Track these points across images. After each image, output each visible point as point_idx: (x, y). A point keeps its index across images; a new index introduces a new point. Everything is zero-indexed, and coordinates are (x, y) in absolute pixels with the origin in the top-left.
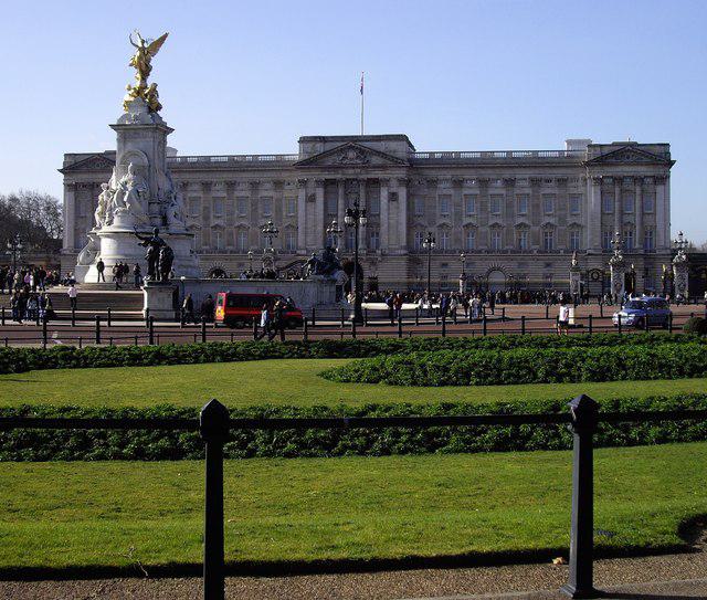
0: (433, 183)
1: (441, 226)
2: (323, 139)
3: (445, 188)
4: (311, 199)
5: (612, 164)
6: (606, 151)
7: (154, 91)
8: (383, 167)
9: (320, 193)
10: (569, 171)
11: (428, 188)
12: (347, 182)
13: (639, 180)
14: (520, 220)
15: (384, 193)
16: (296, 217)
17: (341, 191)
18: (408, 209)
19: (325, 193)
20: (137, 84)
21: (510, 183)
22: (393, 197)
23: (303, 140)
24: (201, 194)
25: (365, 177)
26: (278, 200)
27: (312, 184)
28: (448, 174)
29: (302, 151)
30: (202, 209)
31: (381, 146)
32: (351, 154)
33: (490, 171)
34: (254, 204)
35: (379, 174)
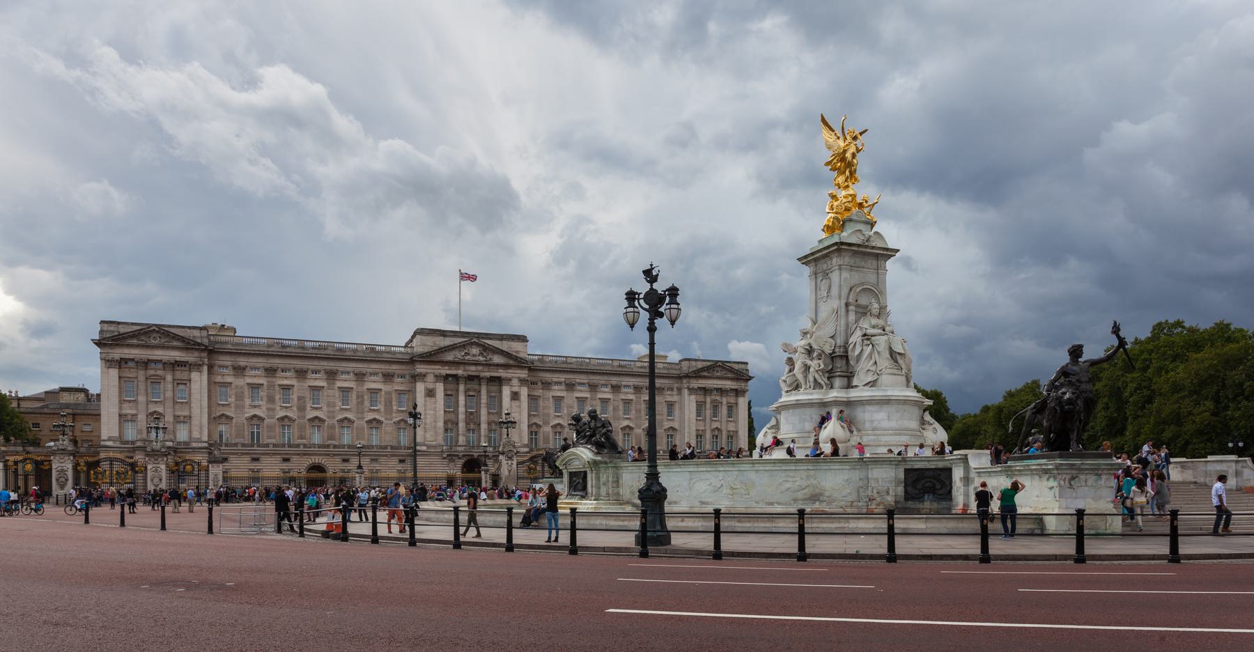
0: (547, 385)
1: (554, 427)
2: (443, 333)
3: (558, 391)
4: (430, 393)
5: (705, 377)
6: (700, 365)
8: (506, 366)
9: (440, 388)
10: (666, 381)
12: (470, 378)
13: (721, 391)
14: (626, 423)
15: (506, 391)
21: (616, 388)
22: (515, 396)
24: (293, 382)
25: (488, 374)
27: (430, 378)
28: (562, 377)
30: (295, 397)
31: (504, 346)
32: (475, 351)
33: (597, 377)
34: (360, 397)
35: (502, 373)
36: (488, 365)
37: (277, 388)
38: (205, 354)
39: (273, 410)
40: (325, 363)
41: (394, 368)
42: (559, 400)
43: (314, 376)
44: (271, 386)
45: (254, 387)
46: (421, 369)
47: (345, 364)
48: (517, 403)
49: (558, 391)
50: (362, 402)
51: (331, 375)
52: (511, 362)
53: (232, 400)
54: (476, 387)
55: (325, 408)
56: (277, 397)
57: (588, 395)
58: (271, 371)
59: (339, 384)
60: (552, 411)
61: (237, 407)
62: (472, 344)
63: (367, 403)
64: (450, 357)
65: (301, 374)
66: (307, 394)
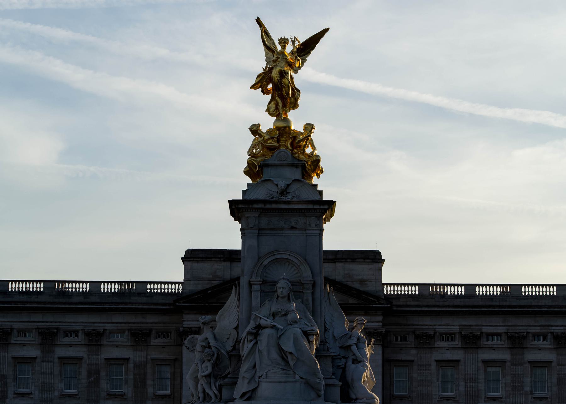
0: (426, 340)
11: (416, 348)
20: (267, 123)
23: (192, 257)
28: (453, 325)
33: (525, 321)
40: (38, 317)
47: (70, 318)
51: (48, 337)
57: (506, 356)
59: (61, 352)
63: (104, 384)
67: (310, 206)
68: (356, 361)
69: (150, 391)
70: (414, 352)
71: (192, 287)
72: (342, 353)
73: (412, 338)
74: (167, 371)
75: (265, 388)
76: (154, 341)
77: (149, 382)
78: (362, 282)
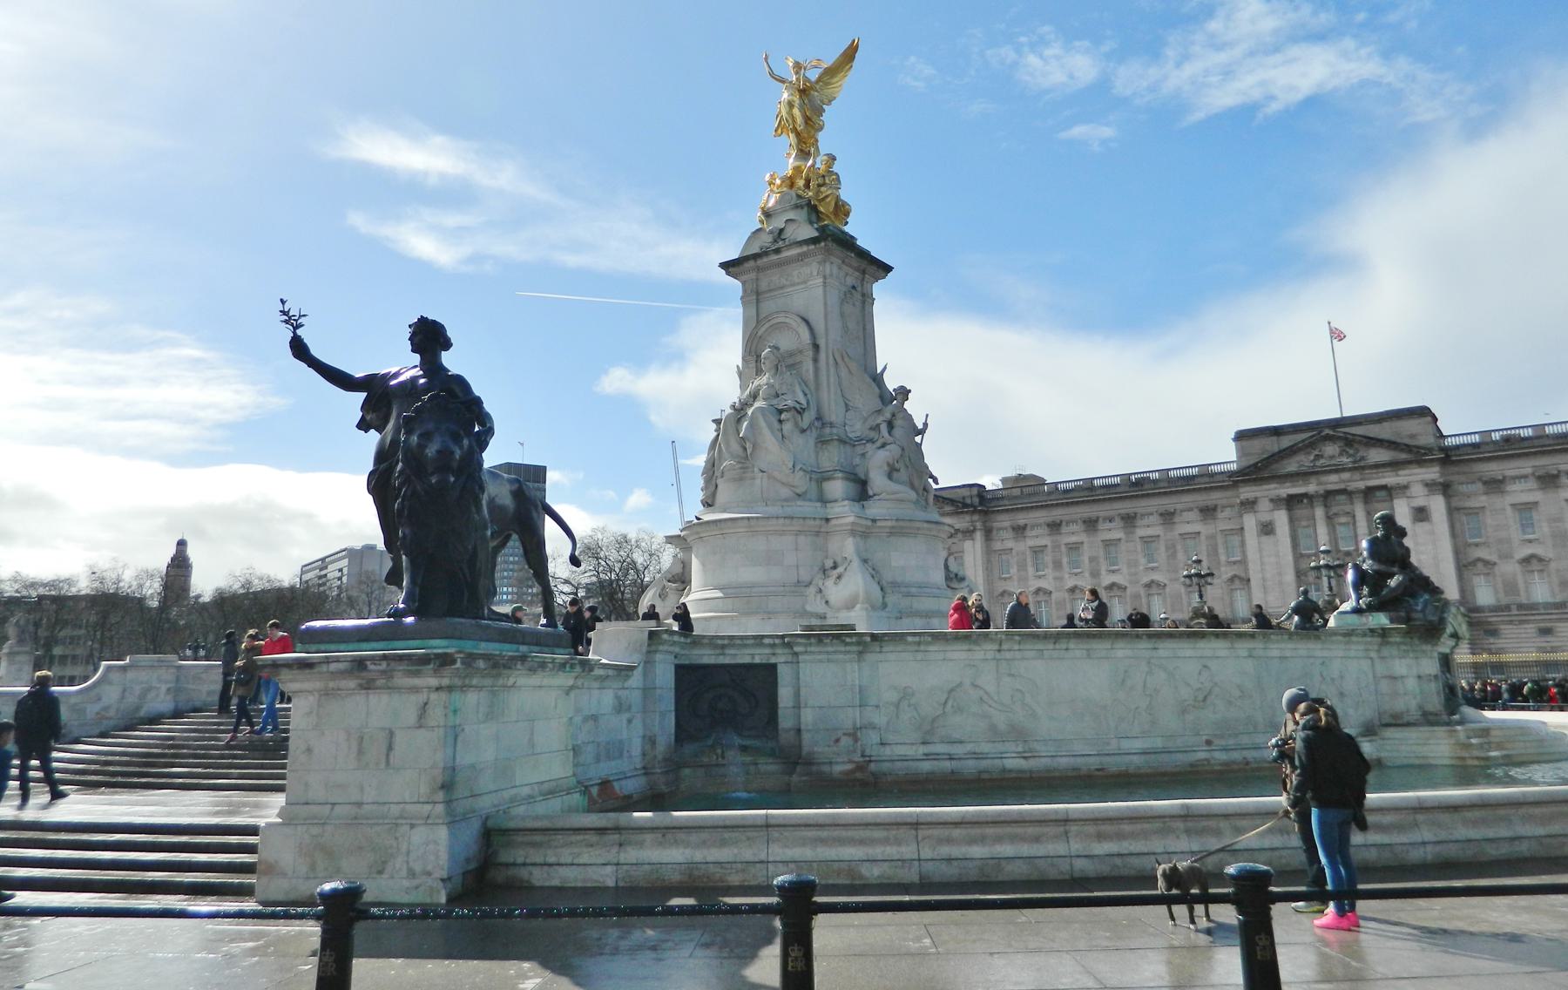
0: (1495, 485)
1: (1527, 560)
2: (1276, 431)
3: (1522, 492)
4: (1267, 529)
7: (828, 178)
8: (1394, 465)
9: (1281, 518)
12: (1328, 496)
16: (1243, 562)
17: (1319, 512)
18: (1453, 535)
19: (1291, 520)
22: (1421, 514)
23: (1242, 436)
24: (1083, 537)
25: (1361, 485)
26: (1212, 537)
27: (1264, 505)
28: (1526, 466)
29: (1242, 453)
30: (1086, 559)
32: (1330, 449)
34: (1172, 550)
35: (1389, 479)
36: (1359, 468)
37: (1063, 548)
38: (976, 517)
39: (1060, 579)
41: (1215, 497)
42: (1525, 509)
43: (1108, 525)
44: (1056, 547)
45: (1037, 551)
46: (1247, 492)
48: (1425, 526)
49: (1522, 492)
50: (1173, 555)
51: (1129, 520)
52: (1403, 456)
53: (1014, 571)
54: (1347, 508)
55: (1125, 570)
56: (1065, 560)
58: (1055, 527)
60: (1515, 534)
61: (1020, 580)
62: (1328, 438)
63: (1181, 556)
64: (1291, 466)
65: (1091, 524)
66: (1101, 553)
67: (805, 248)
68: (883, 446)
69: (1223, 558)
70: (1484, 498)
71: (1245, 463)
72: (872, 434)
73: (1480, 485)
74: (1236, 540)
75: (725, 492)
76: (1220, 515)
77: (1221, 550)
78: (1412, 436)
